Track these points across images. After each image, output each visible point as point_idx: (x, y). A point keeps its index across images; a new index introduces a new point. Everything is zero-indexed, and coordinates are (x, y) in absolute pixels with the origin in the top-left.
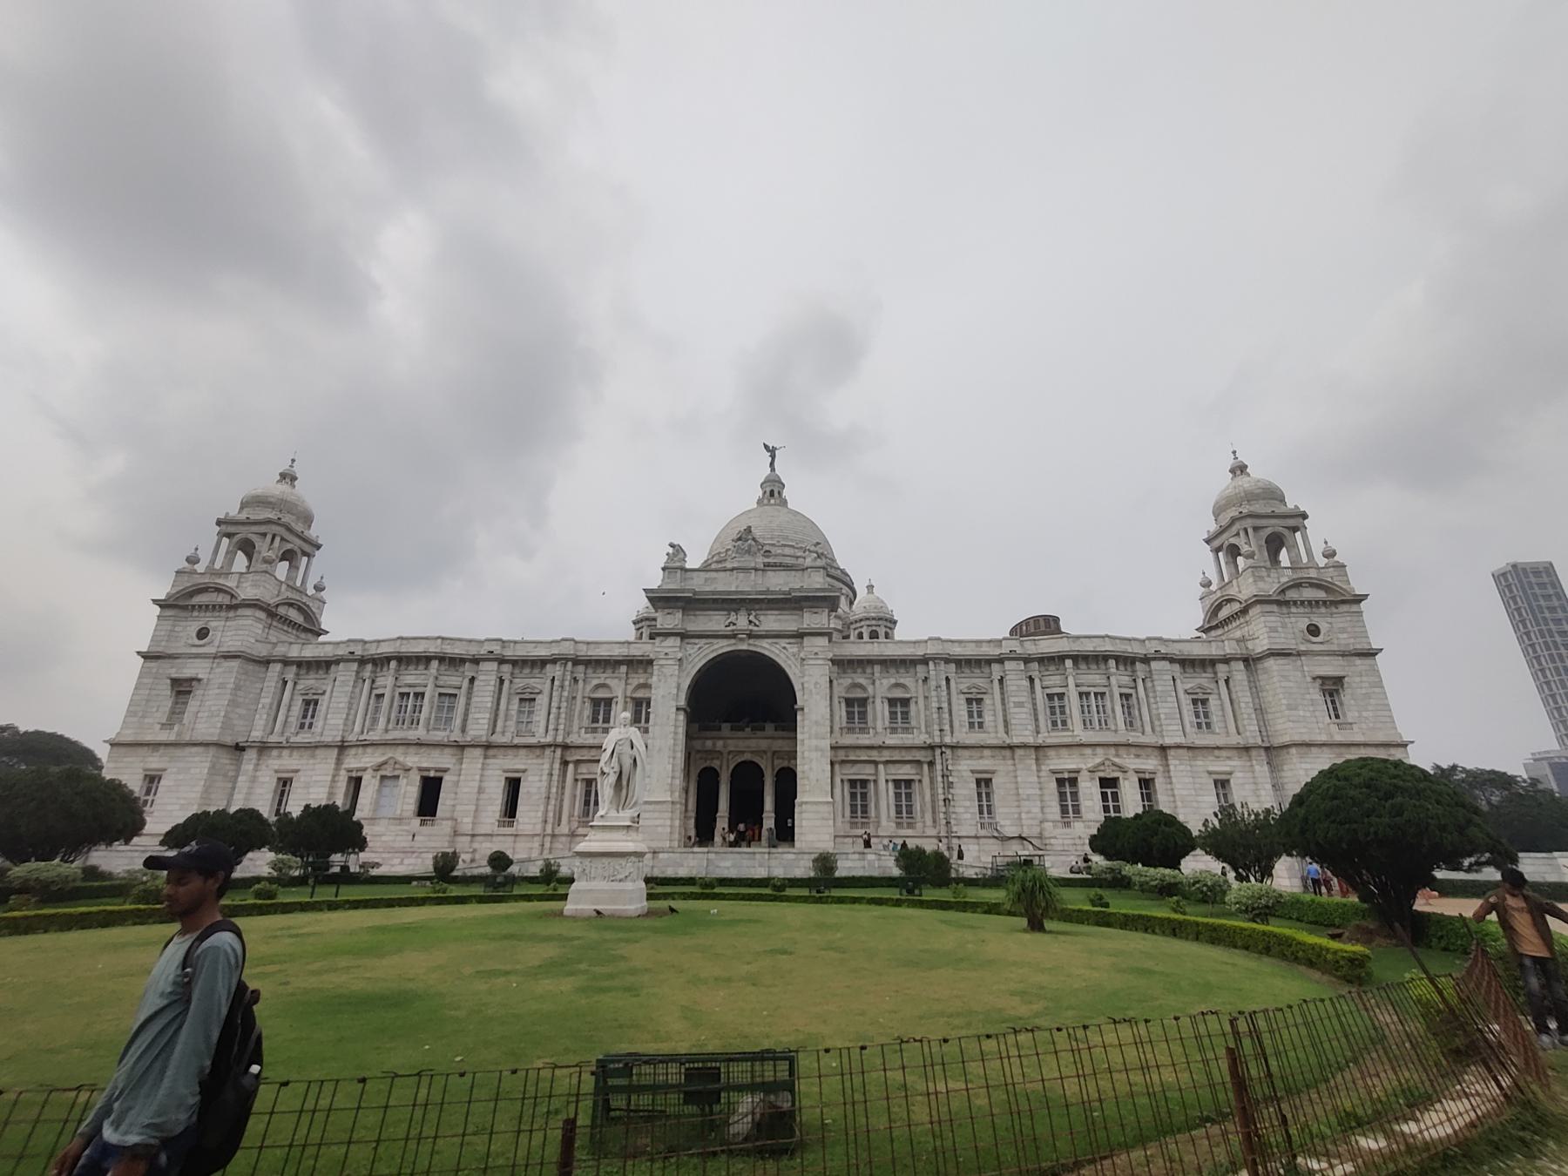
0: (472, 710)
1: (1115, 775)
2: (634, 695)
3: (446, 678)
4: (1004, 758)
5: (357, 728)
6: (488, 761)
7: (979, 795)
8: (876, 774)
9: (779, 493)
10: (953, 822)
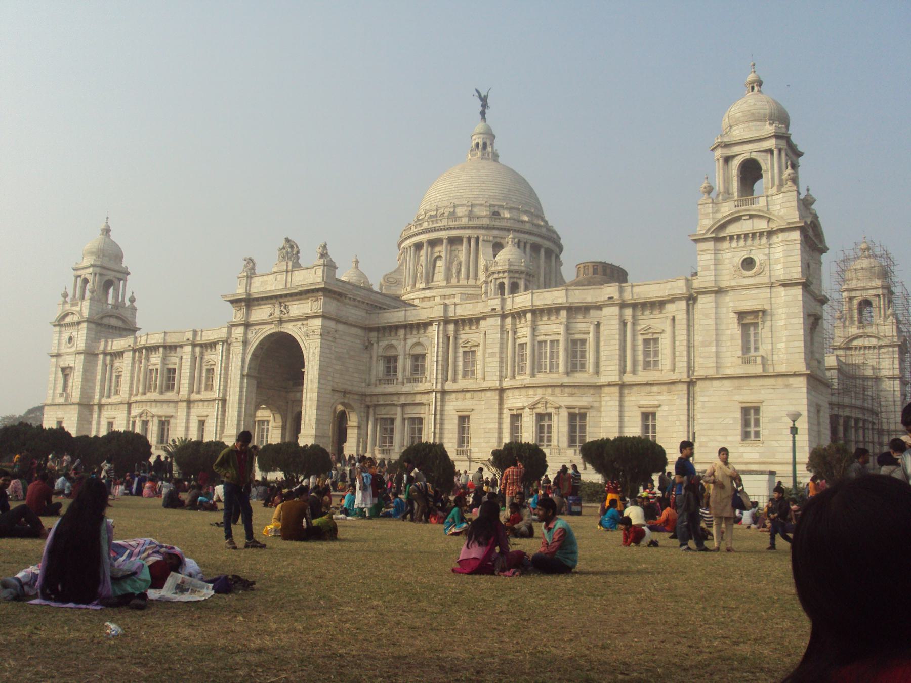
1: (549, 411)
6: (192, 410)
9: (491, 144)
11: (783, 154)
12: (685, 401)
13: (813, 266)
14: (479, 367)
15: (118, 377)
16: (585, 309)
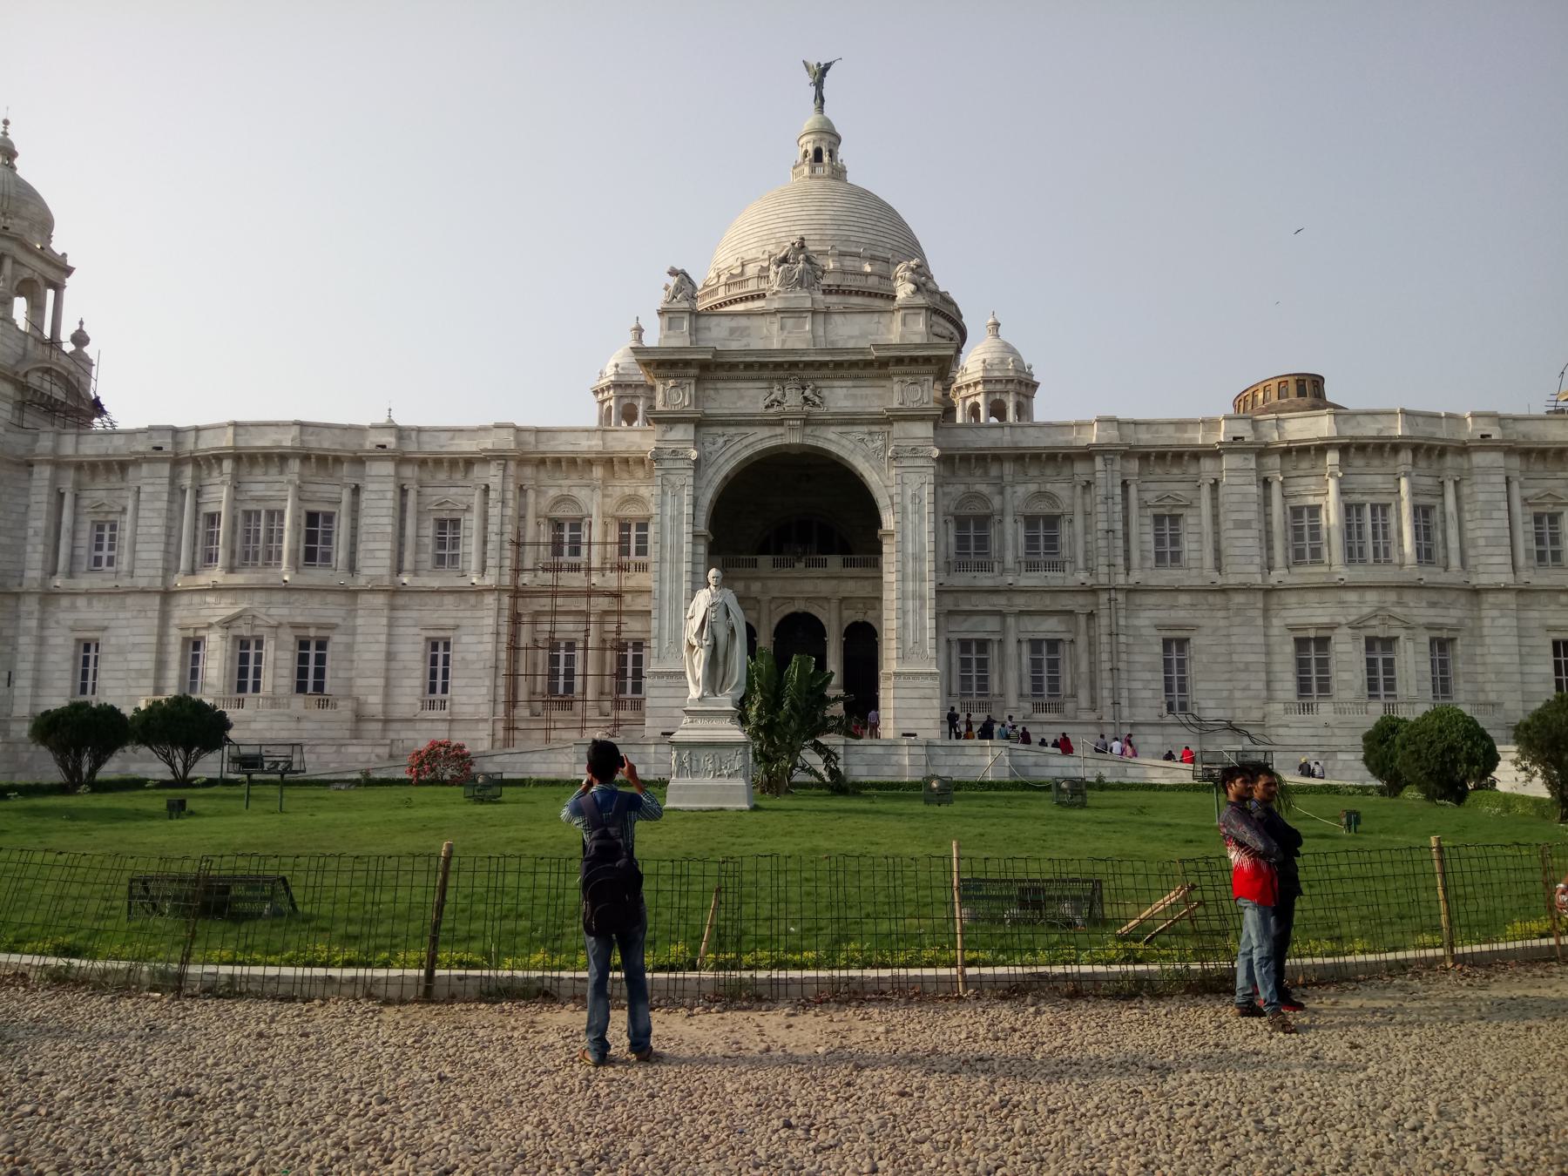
0: (362, 537)
1: (1394, 633)
2: (619, 513)
3: (314, 488)
4: (1212, 608)
5: (183, 565)
6: (400, 614)
7: (1167, 663)
8: (1004, 630)
9: (831, 154)
10: (1124, 702)
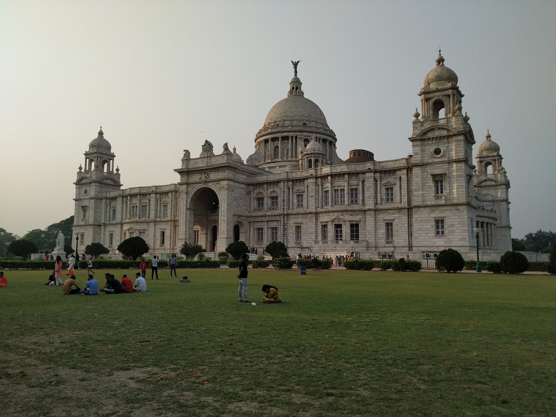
1: (341, 223)
3: (143, 200)
6: (157, 226)
9: (300, 88)
11: (455, 96)
12: (407, 217)
13: (468, 151)
14: (304, 202)
15: (114, 211)
16: (358, 174)
